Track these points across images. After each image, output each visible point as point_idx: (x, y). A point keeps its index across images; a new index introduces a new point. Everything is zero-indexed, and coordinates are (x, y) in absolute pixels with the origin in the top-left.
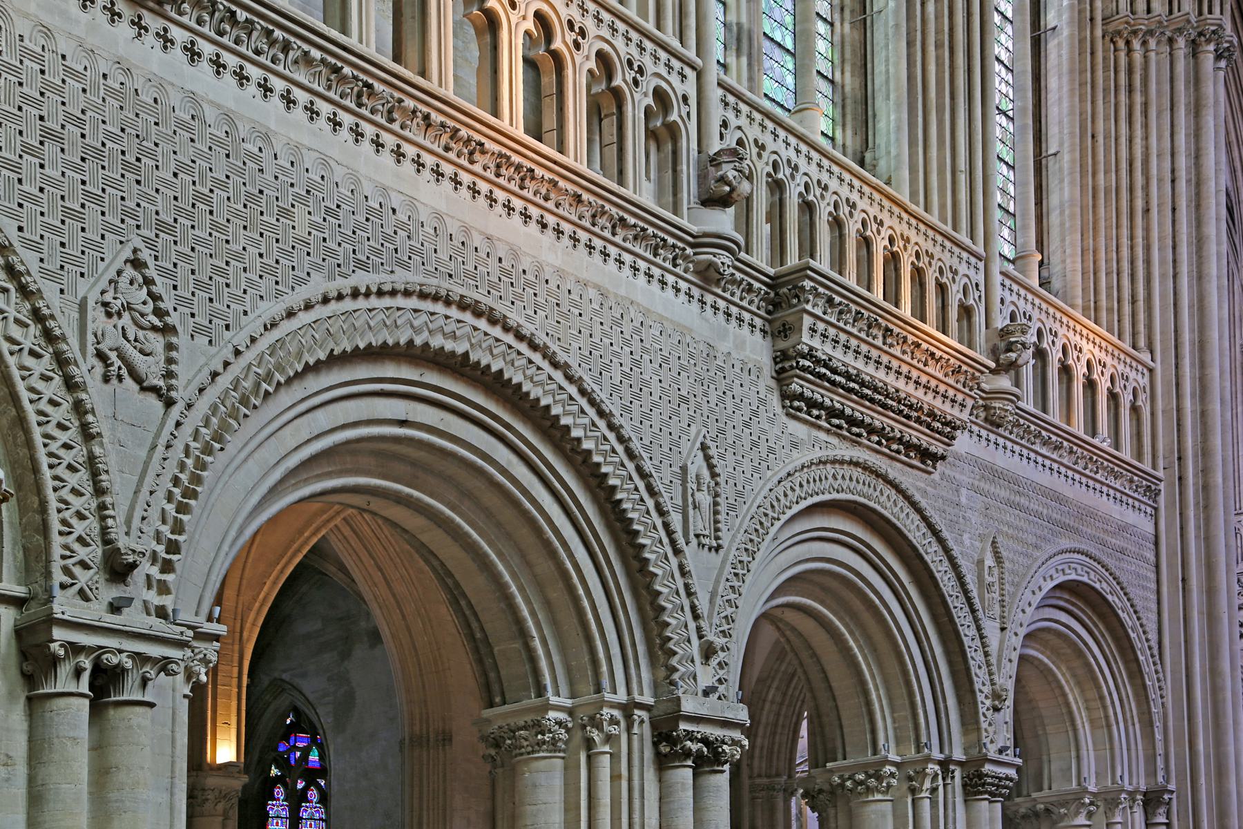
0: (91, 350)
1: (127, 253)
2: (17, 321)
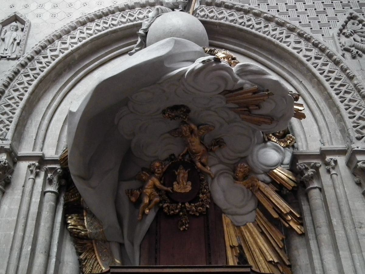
0: (340, 48)
1: (348, 15)
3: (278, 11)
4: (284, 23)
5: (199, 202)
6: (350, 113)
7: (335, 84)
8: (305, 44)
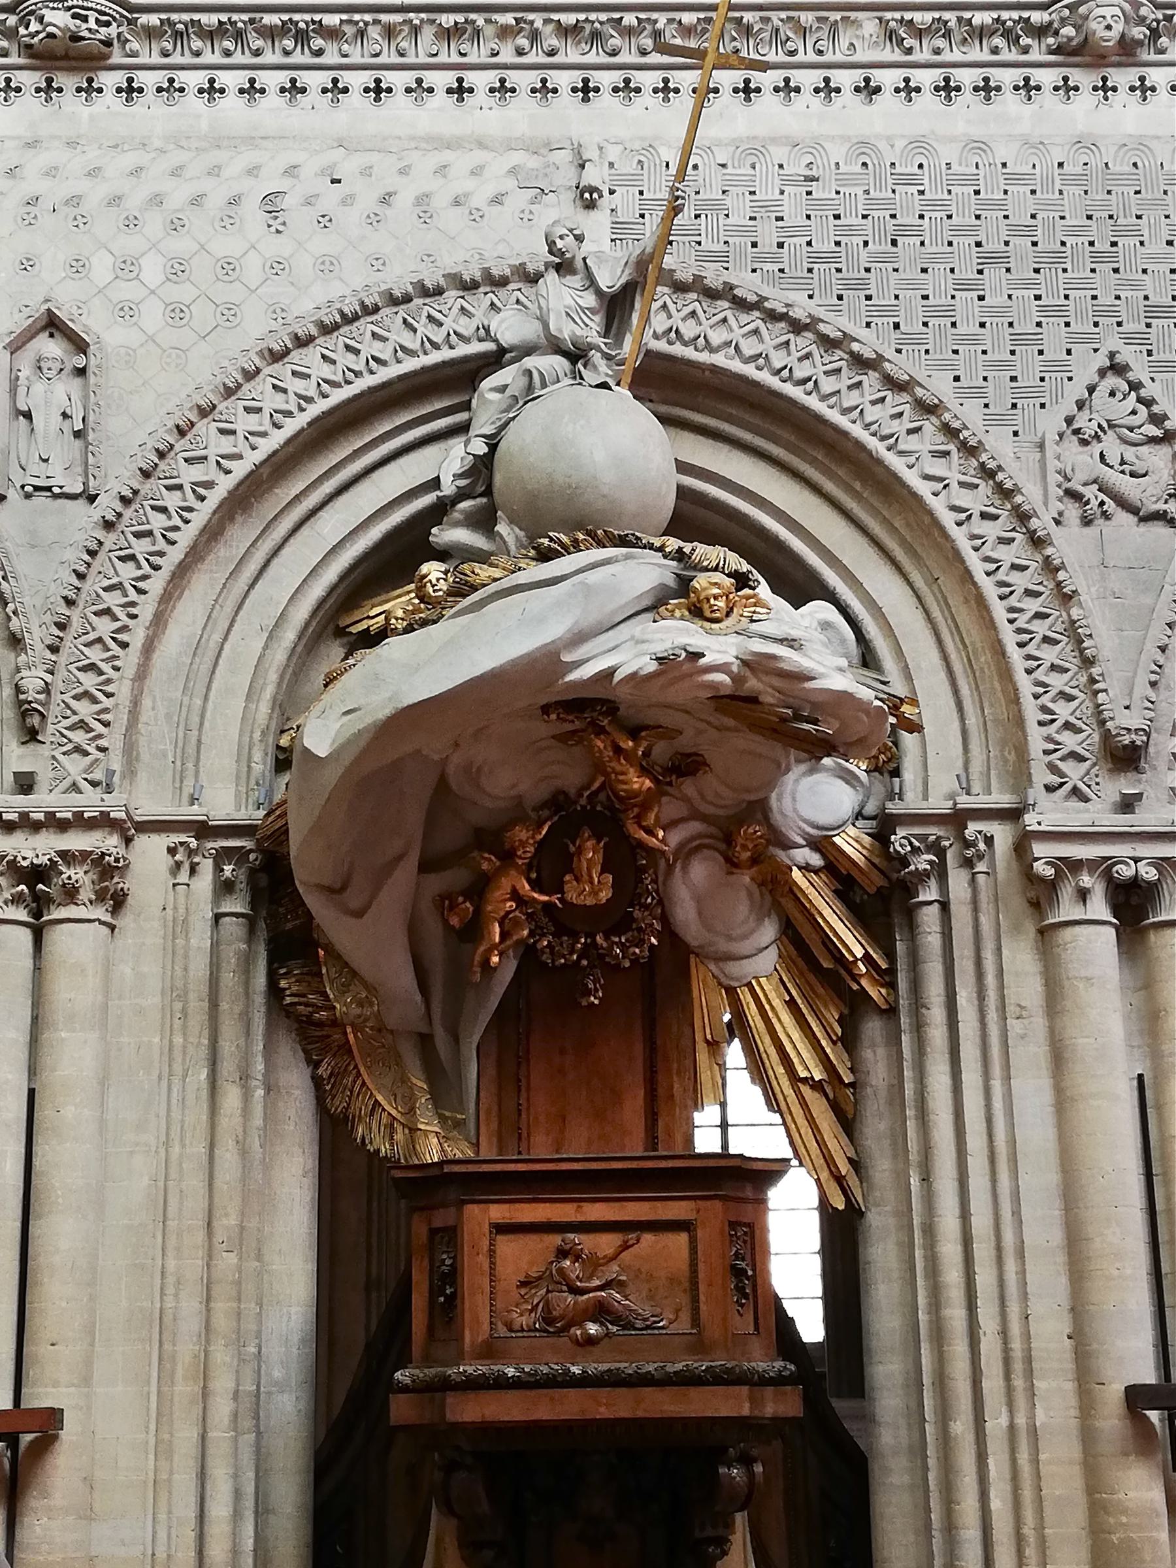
1: (1103, 360)
2: (962, 484)
3: (897, 326)
4: (908, 383)
5: (633, 930)
6: (1044, 709)
7: (1021, 610)
8: (962, 461)
